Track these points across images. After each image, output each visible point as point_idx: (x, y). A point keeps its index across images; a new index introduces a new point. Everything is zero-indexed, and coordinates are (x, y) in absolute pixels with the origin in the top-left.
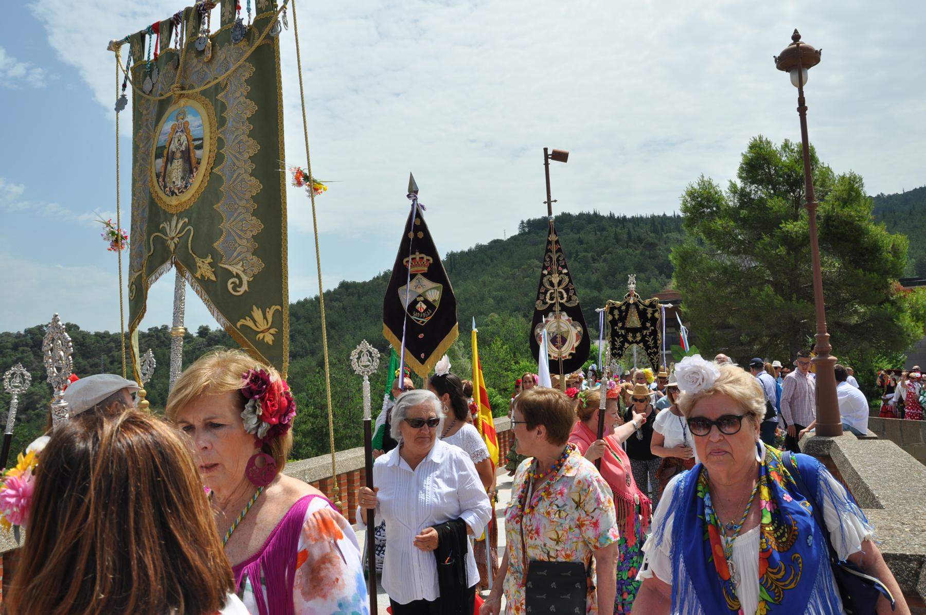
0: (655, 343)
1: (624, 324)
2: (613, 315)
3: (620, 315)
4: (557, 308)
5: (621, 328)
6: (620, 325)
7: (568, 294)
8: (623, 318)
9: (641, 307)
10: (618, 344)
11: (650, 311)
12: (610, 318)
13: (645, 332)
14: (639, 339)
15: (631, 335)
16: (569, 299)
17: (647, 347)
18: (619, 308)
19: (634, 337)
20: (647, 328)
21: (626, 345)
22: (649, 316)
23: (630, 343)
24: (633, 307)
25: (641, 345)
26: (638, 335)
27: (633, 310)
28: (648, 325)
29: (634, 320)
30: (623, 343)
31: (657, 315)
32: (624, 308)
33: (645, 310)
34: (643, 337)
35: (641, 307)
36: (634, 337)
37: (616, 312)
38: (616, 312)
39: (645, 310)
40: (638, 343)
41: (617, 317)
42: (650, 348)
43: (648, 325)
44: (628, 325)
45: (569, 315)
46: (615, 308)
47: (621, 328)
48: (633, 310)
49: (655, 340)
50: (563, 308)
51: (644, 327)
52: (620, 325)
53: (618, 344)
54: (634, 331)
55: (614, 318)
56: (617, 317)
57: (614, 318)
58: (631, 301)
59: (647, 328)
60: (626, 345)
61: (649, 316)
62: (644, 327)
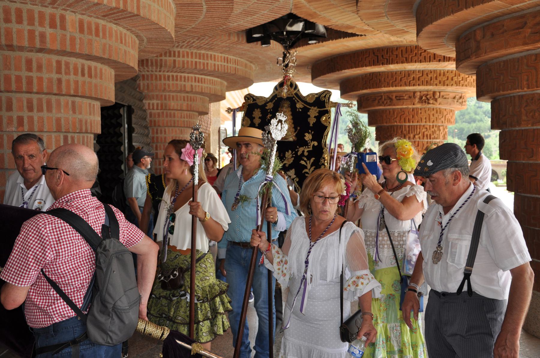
9: (299, 105)
11: (313, 112)
13: (301, 150)
20: (306, 144)
22: (312, 121)
24: (286, 104)
26: (289, 154)
28: (308, 137)
33: (305, 110)
34: (298, 158)
35: (299, 105)
43: (308, 137)
51: (300, 141)
59: (306, 144)
61: (312, 121)
62: (300, 141)
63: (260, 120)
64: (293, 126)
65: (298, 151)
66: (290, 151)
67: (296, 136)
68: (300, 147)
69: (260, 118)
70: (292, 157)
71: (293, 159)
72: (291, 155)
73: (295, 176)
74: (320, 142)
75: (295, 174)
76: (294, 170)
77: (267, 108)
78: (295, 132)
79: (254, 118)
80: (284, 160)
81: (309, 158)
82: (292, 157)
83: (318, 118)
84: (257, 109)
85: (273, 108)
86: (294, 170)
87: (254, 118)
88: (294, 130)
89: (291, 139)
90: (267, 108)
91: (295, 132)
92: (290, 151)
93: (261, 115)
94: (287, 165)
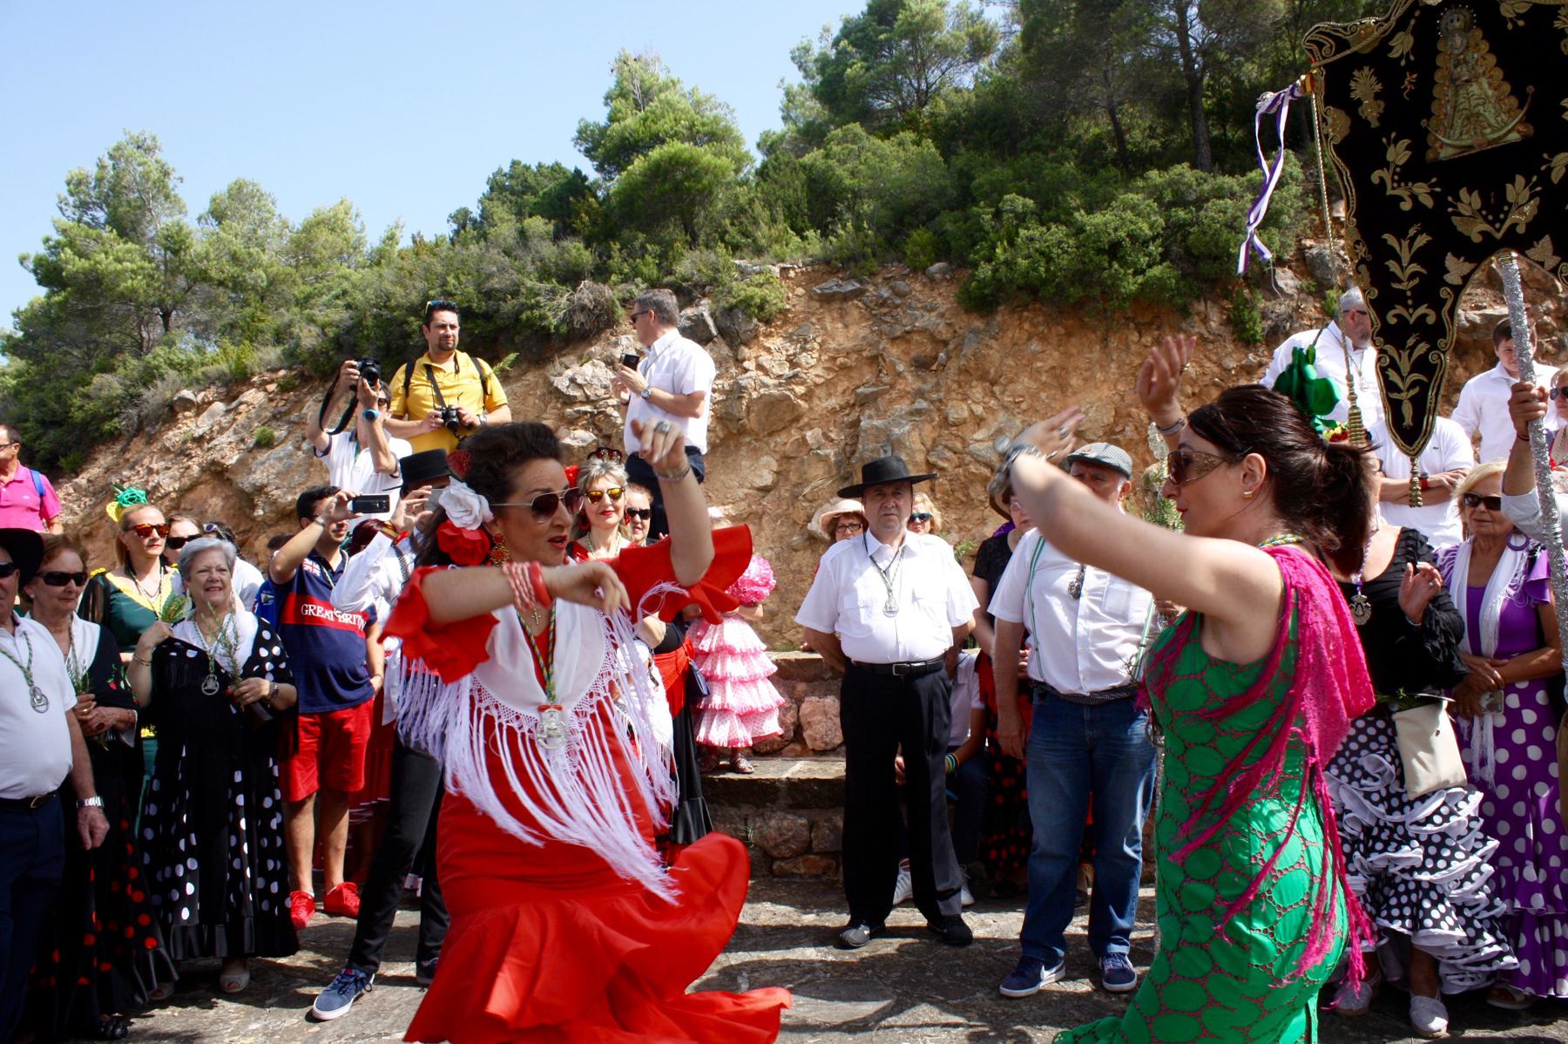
1: (1420, 145)
5: (1409, 173)
6: (1398, 154)
8: (1410, 110)
10: (1405, 270)
15: (1469, 201)
18: (1378, 57)
21: (1455, 268)
23: (1478, 253)
26: (1517, 190)
30: (1431, 259)
32: (1402, 45)
36: (1495, 207)
37: (1364, 85)
38: (1364, 85)
40: (1520, 242)
41: (1371, 111)
44: (1446, 145)
46: (1357, 61)
47: (1409, 173)
52: (1398, 154)
53: (1405, 270)
54: (1487, 170)
55: (1358, 124)
56: (1371, 111)
57: (1358, 124)
60: (1455, 268)
63: (1382, 104)
64: (1507, 87)
65: (1550, 170)
66: (1520, 180)
67: (1527, 119)
68: (1552, 155)
69: (1377, 96)
70: (1532, 197)
71: (1535, 202)
72: (1527, 193)
73: (1557, 259)
75: (1555, 253)
76: (1547, 237)
77: (1394, 55)
78: (1521, 107)
79: (1359, 102)
80: (1507, 214)
82: (1532, 197)
84: (1361, 69)
85: (1414, 50)
86: (1547, 237)
87: (1359, 102)
88: (1514, 101)
89: (1514, 137)
90: (1394, 55)
91: (1521, 107)
92: (1520, 180)
93: (1378, 87)
94: (1521, 230)
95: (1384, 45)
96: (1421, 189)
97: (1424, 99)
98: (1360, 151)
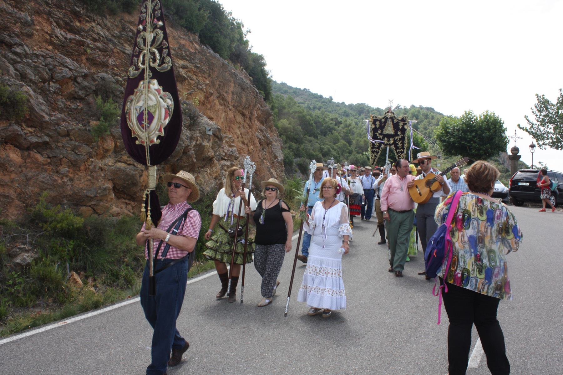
0: (403, 146)
1: (382, 131)
2: (375, 125)
3: (380, 125)
4: (148, 74)
5: (380, 134)
6: (379, 132)
7: (161, 56)
8: (382, 127)
9: (395, 121)
11: (401, 124)
12: (373, 127)
13: (396, 138)
14: (392, 142)
15: (386, 139)
16: (162, 62)
17: (397, 148)
18: (380, 121)
19: (389, 141)
20: (398, 135)
22: (400, 127)
24: (390, 120)
25: (393, 147)
26: (391, 139)
27: (390, 122)
28: (399, 133)
29: (389, 130)
31: (406, 127)
32: (383, 120)
33: (398, 123)
34: (395, 141)
35: (395, 121)
36: (389, 141)
37: (378, 123)
38: (378, 123)
39: (398, 123)
40: (390, 145)
41: (378, 126)
42: (399, 149)
43: (399, 133)
44: (386, 132)
45: (160, 84)
47: (380, 134)
48: (390, 122)
49: (403, 144)
50: (156, 74)
52: (379, 132)
54: (389, 136)
55: (376, 127)
56: (378, 126)
58: (389, 117)
59: (398, 135)
61: (400, 127)
74: (404, 135)
81: (399, 141)
83: (403, 126)
95: (381, 120)
96: (381, 136)
97: (384, 127)
98: (375, 130)
